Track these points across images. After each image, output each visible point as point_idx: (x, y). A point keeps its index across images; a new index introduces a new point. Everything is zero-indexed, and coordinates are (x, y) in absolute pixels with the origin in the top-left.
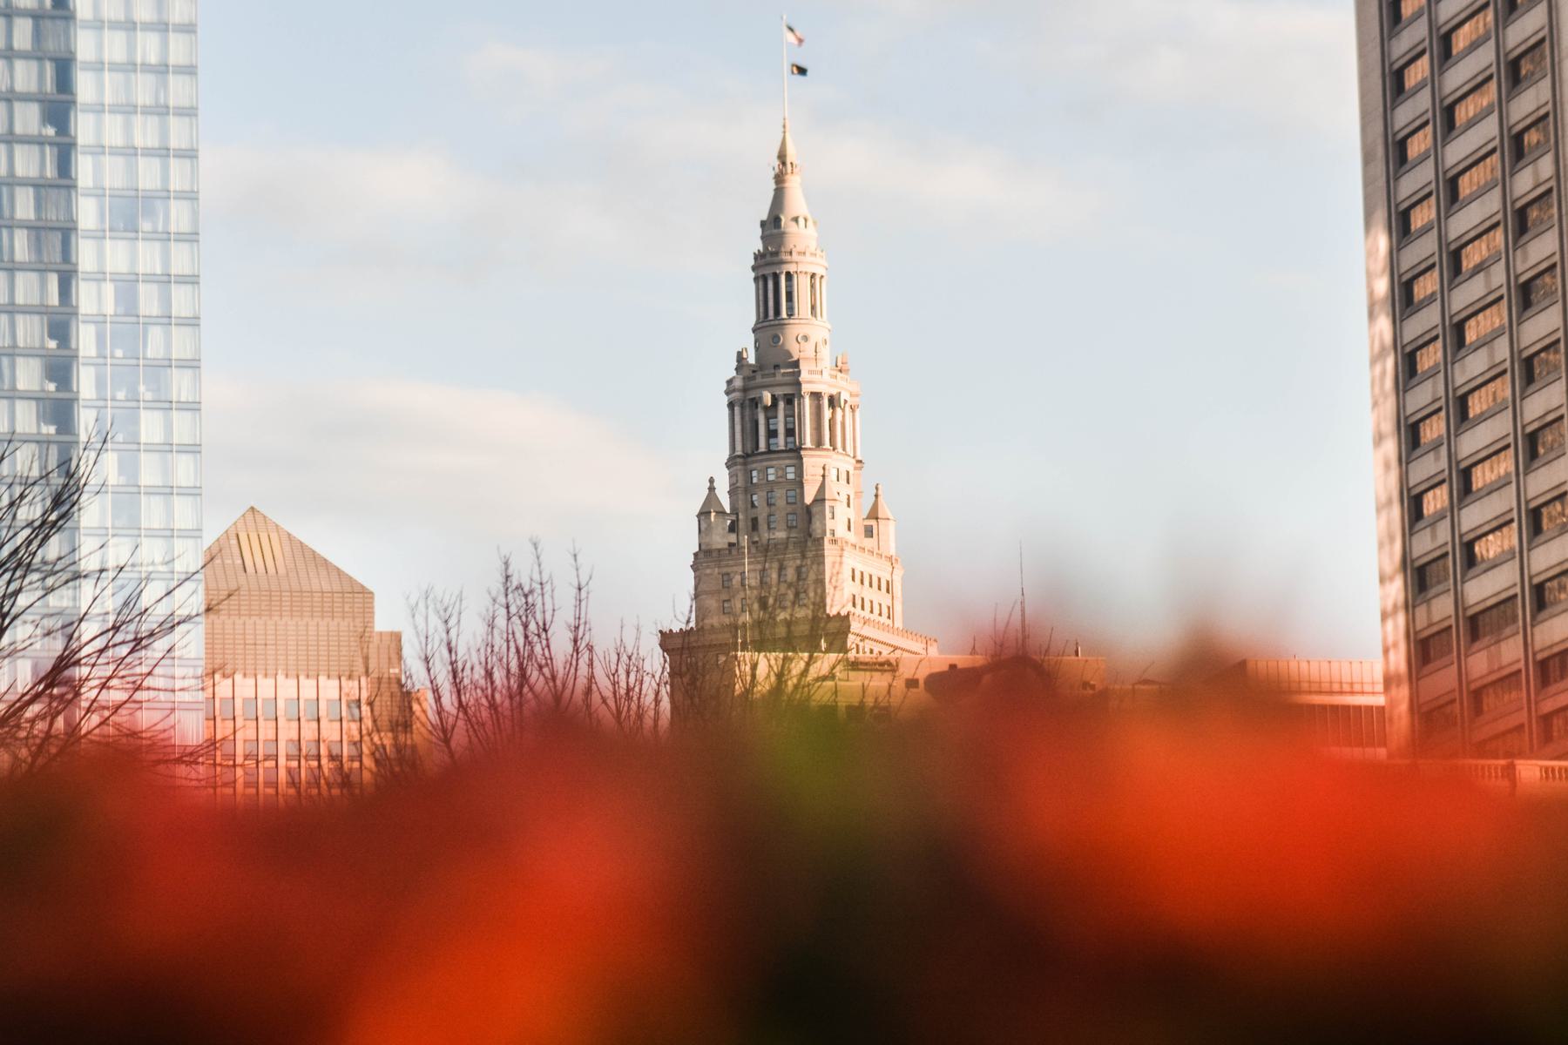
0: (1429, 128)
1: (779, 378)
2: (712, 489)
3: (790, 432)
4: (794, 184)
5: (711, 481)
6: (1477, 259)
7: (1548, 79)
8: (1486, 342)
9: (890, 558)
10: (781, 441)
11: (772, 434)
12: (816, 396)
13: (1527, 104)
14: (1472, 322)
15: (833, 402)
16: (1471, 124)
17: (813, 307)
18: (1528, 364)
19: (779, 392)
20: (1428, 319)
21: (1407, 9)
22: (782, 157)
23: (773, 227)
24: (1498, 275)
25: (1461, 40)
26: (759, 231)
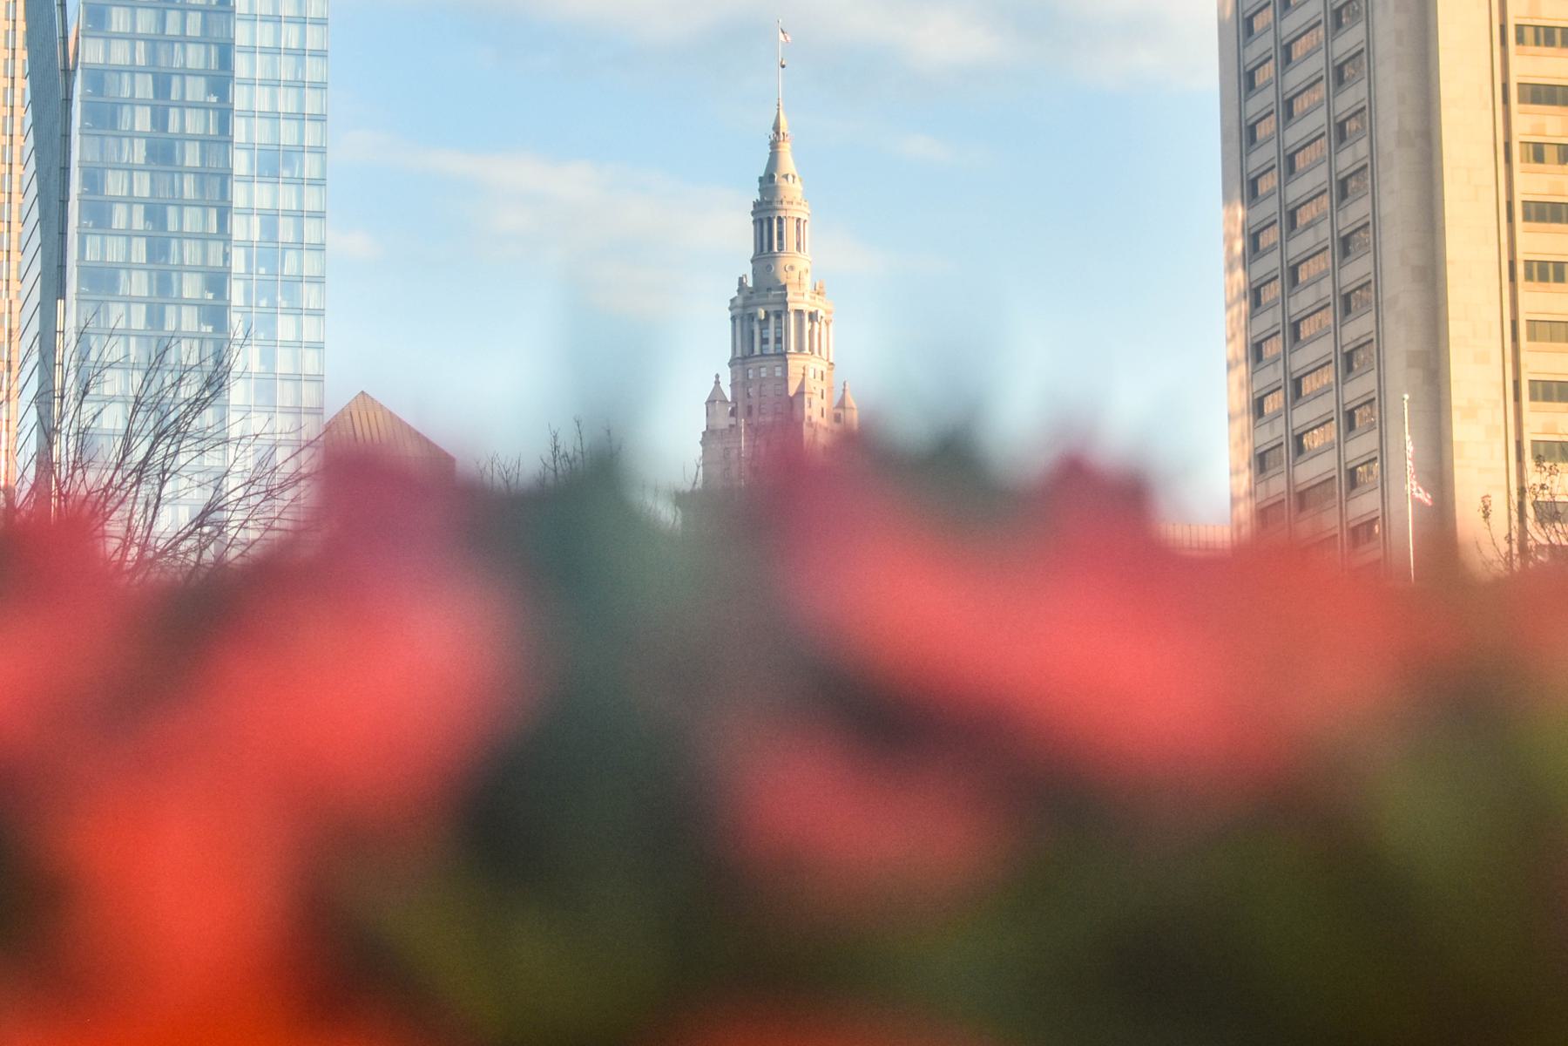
0: (1273, 117)
1: (771, 298)
2: (717, 383)
3: (778, 340)
4: (786, 149)
6: (1308, 218)
7: (1365, 82)
8: (1315, 281)
11: (765, 341)
12: (799, 313)
13: (1347, 101)
14: (1304, 266)
16: (1305, 114)
17: (798, 244)
18: (1347, 298)
19: (771, 309)
20: (1270, 263)
22: (776, 128)
23: (768, 182)
24: (1324, 230)
25: (1298, 51)
26: (758, 185)
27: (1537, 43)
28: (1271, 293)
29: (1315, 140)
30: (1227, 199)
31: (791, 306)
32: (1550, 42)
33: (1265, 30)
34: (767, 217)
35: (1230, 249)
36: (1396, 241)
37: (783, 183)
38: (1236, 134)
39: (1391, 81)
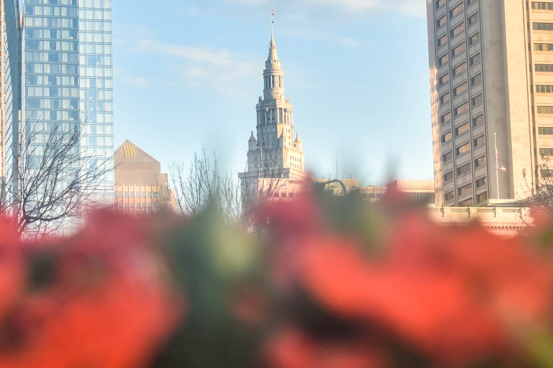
0: (447, 36)
2: (252, 134)
3: (273, 119)
4: (274, 51)
5: (252, 132)
8: (462, 94)
9: (300, 153)
10: (271, 121)
11: (269, 119)
12: (281, 109)
13: (473, 30)
14: (458, 88)
15: (285, 110)
16: (458, 35)
17: (280, 85)
19: (271, 108)
20: (446, 88)
21: (441, 4)
22: (271, 44)
24: (465, 76)
25: (455, 13)
27: (539, 8)
28: (447, 98)
29: (461, 44)
30: (431, 66)
31: (278, 107)
32: (544, 8)
33: (443, 6)
34: (268, 76)
35: (433, 83)
36: (490, 79)
37: (274, 63)
38: (433, 43)
39: (488, 22)
